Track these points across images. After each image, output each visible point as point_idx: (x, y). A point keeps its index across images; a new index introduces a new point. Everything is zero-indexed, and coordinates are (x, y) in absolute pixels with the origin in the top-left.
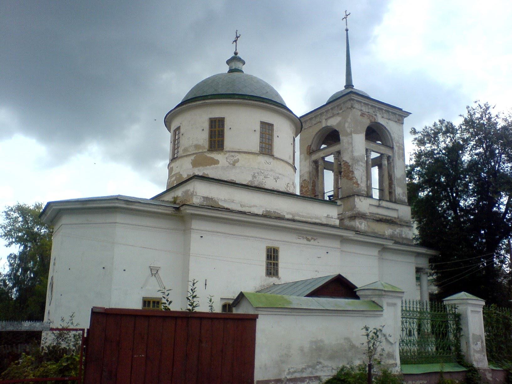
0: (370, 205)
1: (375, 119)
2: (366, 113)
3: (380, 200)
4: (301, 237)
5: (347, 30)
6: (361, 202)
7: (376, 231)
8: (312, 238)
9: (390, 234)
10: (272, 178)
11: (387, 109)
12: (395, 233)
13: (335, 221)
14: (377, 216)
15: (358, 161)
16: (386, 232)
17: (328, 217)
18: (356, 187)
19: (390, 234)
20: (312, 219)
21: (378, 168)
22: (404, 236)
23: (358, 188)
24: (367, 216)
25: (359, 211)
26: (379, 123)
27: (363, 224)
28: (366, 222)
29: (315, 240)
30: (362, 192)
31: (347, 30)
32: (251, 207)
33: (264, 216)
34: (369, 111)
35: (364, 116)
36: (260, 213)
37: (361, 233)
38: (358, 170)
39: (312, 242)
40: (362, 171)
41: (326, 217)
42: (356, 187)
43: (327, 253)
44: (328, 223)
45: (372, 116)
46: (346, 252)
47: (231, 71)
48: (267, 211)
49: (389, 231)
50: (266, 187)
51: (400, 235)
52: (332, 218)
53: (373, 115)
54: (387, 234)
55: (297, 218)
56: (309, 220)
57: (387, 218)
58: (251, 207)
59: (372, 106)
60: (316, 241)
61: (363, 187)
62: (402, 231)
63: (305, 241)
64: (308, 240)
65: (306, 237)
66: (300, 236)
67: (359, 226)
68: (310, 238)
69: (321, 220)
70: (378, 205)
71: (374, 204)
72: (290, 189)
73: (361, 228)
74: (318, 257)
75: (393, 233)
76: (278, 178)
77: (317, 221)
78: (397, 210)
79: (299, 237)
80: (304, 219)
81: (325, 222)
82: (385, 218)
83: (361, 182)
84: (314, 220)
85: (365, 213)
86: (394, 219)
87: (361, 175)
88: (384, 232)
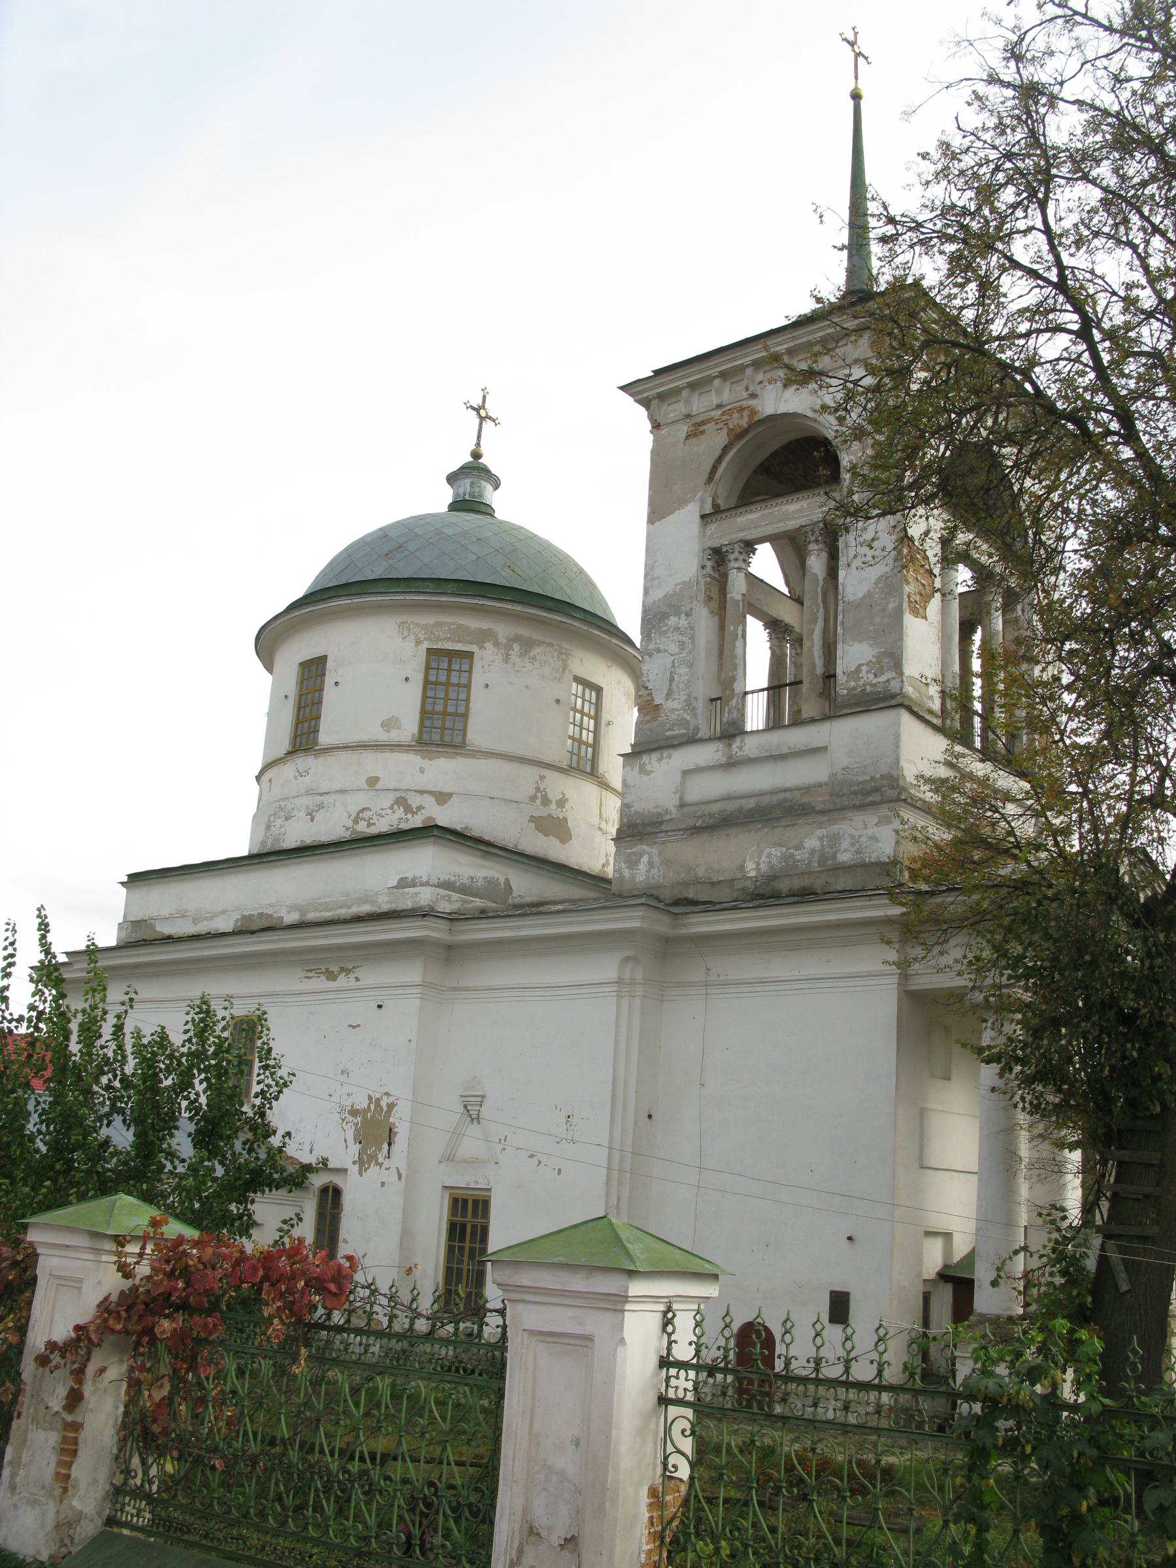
0: (685, 773)
1: (753, 412)
2: (713, 413)
3: (768, 729)
4: (313, 974)
5: (856, 96)
6: (645, 777)
7: (701, 872)
8: (342, 969)
9: (772, 867)
10: (302, 814)
11: (792, 344)
12: (799, 855)
13: (416, 894)
14: (715, 808)
15: (665, 616)
16: (750, 866)
17: (403, 883)
18: (648, 722)
19: (772, 867)
20: (350, 907)
21: (966, 566)
22: (844, 857)
23: (656, 723)
24: (661, 823)
25: (637, 813)
26: (772, 418)
27: (645, 859)
28: (655, 850)
29: (347, 971)
30: (668, 733)
31: (856, 96)
32: (212, 918)
33: (244, 931)
34: (726, 396)
35: (702, 432)
36: (228, 928)
37: (642, 900)
38: (658, 651)
39: (342, 981)
40: (674, 648)
41: (396, 887)
42: (648, 722)
43: (380, 1006)
44: (393, 906)
45: (741, 410)
46: (476, 989)
47: (458, 506)
48: (244, 917)
49: (764, 858)
50: (289, 843)
51: (823, 858)
52: (414, 885)
53: (744, 404)
54: (753, 874)
55: (311, 916)
56: (343, 912)
57: (765, 800)
58: (214, 916)
59: (724, 375)
60: (352, 976)
61: (673, 710)
62: (835, 839)
63: (321, 983)
64: (331, 976)
65: (327, 969)
66: (310, 971)
67: (626, 873)
68: (335, 968)
69: (373, 903)
70: (723, 760)
71: (702, 763)
72: (369, 825)
73: (633, 878)
74: (354, 1027)
75: (786, 857)
76: (321, 806)
77: (366, 908)
78: (821, 750)
79: (309, 974)
80: (328, 915)
81: (386, 907)
82: (750, 804)
83: (669, 695)
84: (356, 910)
85: (660, 815)
86: (797, 794)
87: (669, 666)
88: (742, 868)
